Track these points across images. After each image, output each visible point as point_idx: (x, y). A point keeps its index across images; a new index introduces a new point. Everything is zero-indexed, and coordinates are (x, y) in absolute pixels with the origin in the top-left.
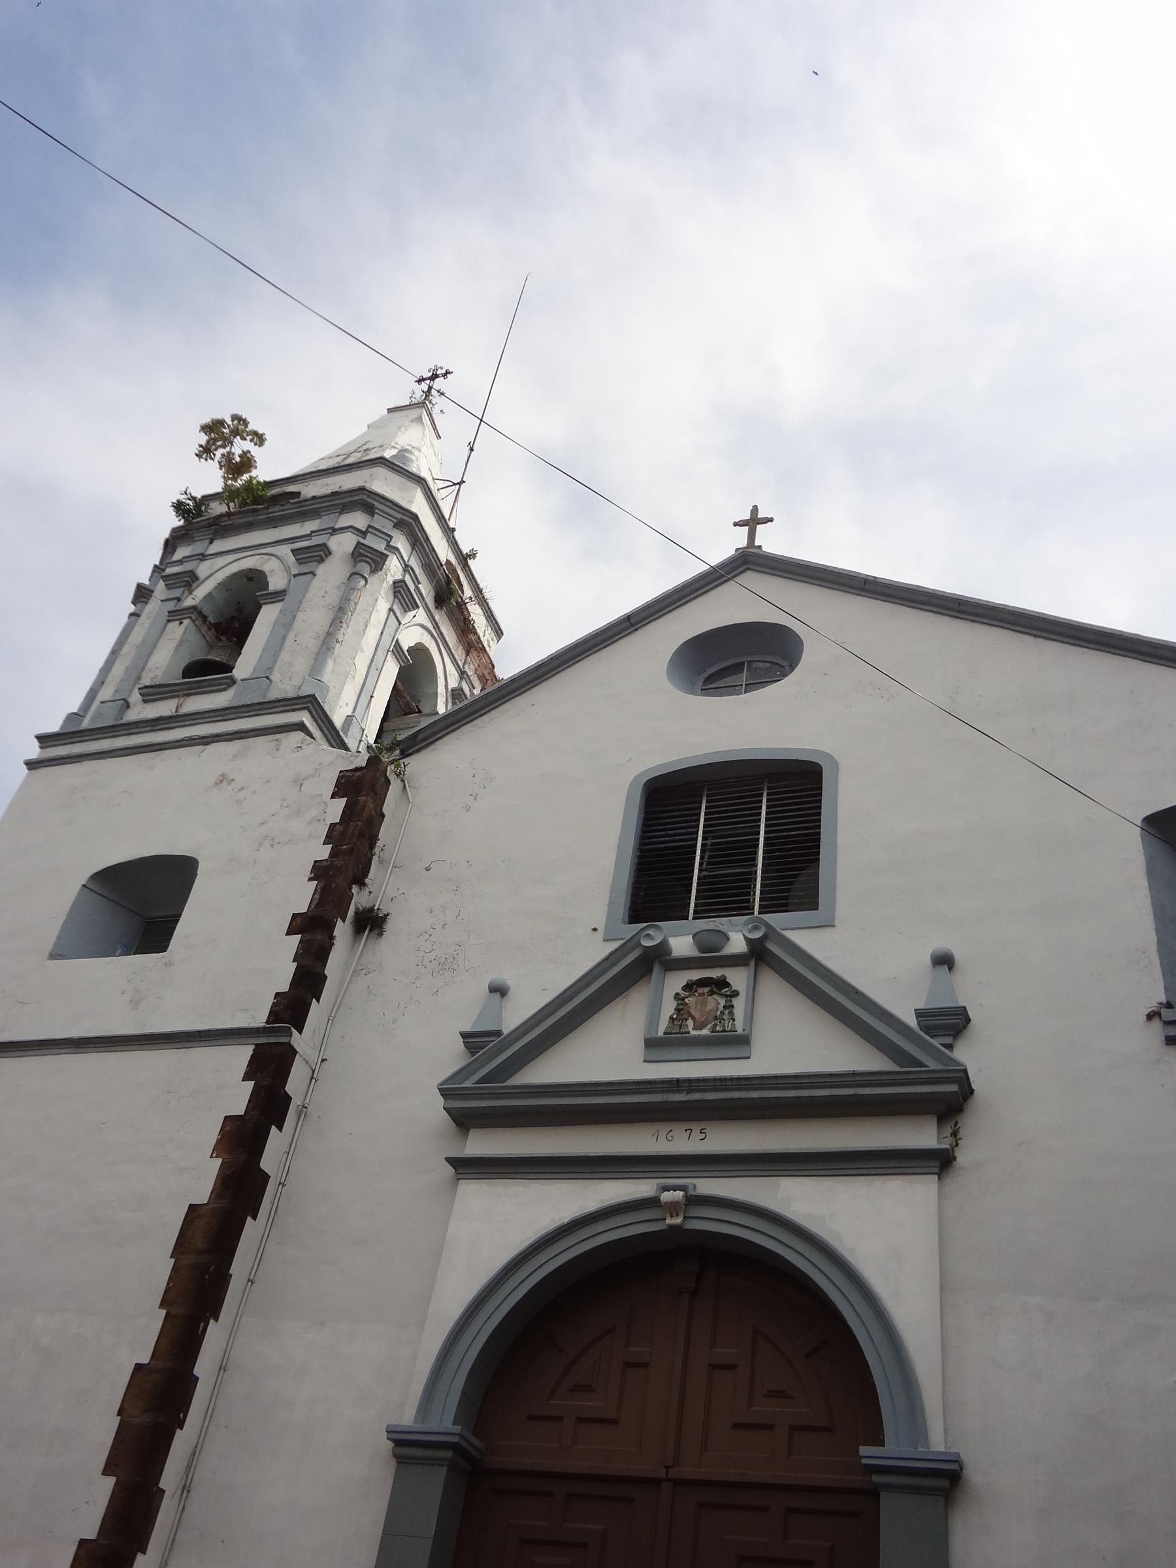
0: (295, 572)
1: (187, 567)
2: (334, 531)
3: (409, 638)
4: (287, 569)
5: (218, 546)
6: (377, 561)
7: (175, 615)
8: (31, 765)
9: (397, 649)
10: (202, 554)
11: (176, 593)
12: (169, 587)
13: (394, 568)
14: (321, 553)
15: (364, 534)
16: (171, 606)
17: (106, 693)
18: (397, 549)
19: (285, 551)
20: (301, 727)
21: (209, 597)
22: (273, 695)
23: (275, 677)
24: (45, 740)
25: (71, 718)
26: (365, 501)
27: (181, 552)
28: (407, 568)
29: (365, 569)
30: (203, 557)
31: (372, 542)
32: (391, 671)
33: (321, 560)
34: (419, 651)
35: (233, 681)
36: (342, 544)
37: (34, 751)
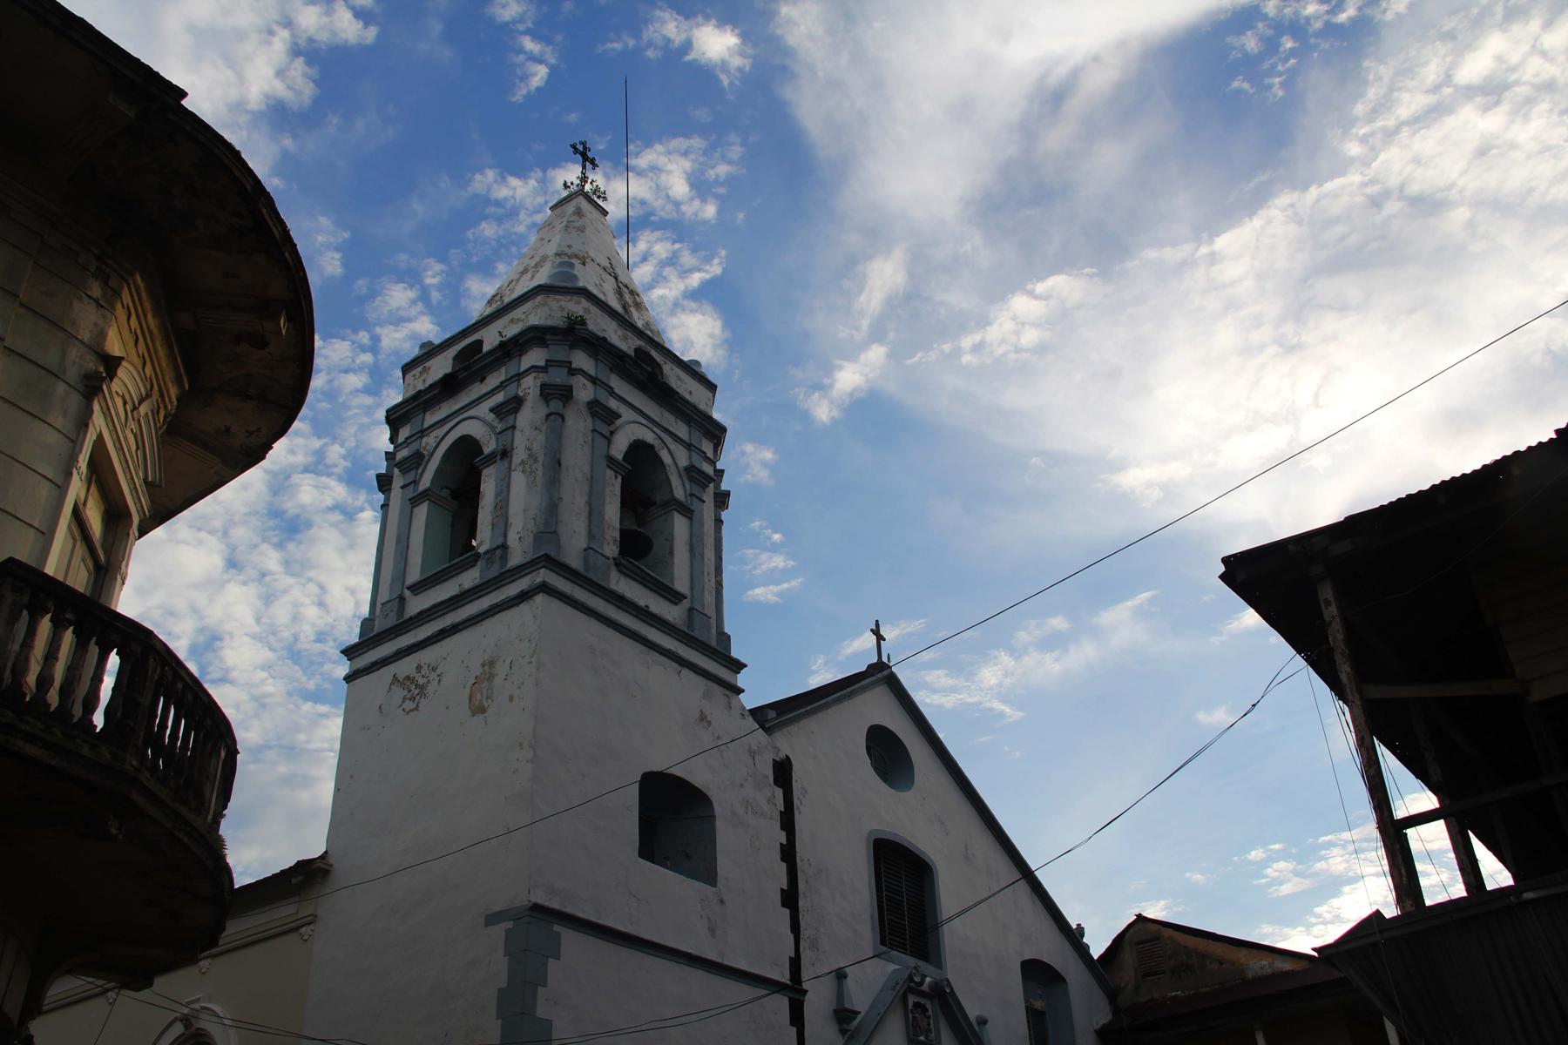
0: (500, 427)
1: (414, 446)
2: (519, 376)
3: (620, 447)
4: (493, 428)
5: (430, 419)
6: (565, 394)
7: (415, 501)
8: (349, 679)
9: (611, 461)
10: (422, 431)
11: (410, 477)
12: (404, 472)
13: (584, 392)
14: (516, 403)
15: (544, 369)
16: (410, 493)
17: (384, 596)
18: (581, 371)
19: (483, 410)
20: (544, 588)
21: (439, 470)
22: (515, 560)
23: (509, 543)
24: (350, 652)
25: (366, 624)
26: (535, 336)
27: (404, 433)
28: (594, 380)
29: (556, 405)
30: (423, 433)
31: (558, 376)
32: (613, 487)
33: (516, 410)
34: (639, 450)
35: (478, 556)
36: (530, 385)
37: (343, 668)
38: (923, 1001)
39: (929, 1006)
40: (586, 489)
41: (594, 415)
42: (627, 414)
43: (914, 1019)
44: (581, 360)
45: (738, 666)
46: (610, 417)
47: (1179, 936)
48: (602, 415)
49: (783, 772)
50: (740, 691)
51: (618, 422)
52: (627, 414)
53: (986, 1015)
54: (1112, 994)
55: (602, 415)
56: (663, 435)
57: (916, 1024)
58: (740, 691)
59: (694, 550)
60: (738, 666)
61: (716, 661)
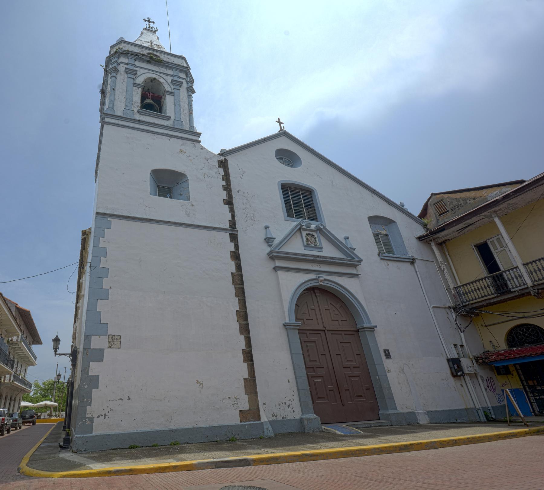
3: (140, 80)
6: (116, 70)
9: (135, 85)
13: (122, 68)
38: (311, 233)
39: (315, 234)
40: (125, 93)
41: (127, 73)
42: (140, 71)
43: (307, 239)
44: (122, 59)
45: (199, 135)
46: (135, 73)
47: (451, 195)
48: (132, 73)
49: (223, 164)
50: (200, 142)
51: (139, 73)
52: (142, 71)
53: (347, 235)
54: (425, 226)
55: (132, 73)
56: (160, 75)
57: (308, 240)
58: (200, 142)
59: (177, 104)
60: (199, 135)
61: (193, 136)
